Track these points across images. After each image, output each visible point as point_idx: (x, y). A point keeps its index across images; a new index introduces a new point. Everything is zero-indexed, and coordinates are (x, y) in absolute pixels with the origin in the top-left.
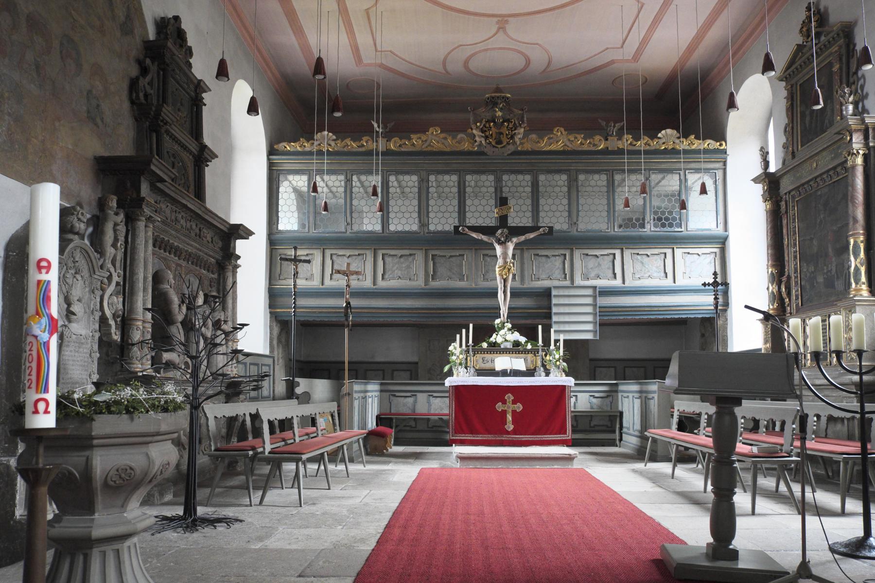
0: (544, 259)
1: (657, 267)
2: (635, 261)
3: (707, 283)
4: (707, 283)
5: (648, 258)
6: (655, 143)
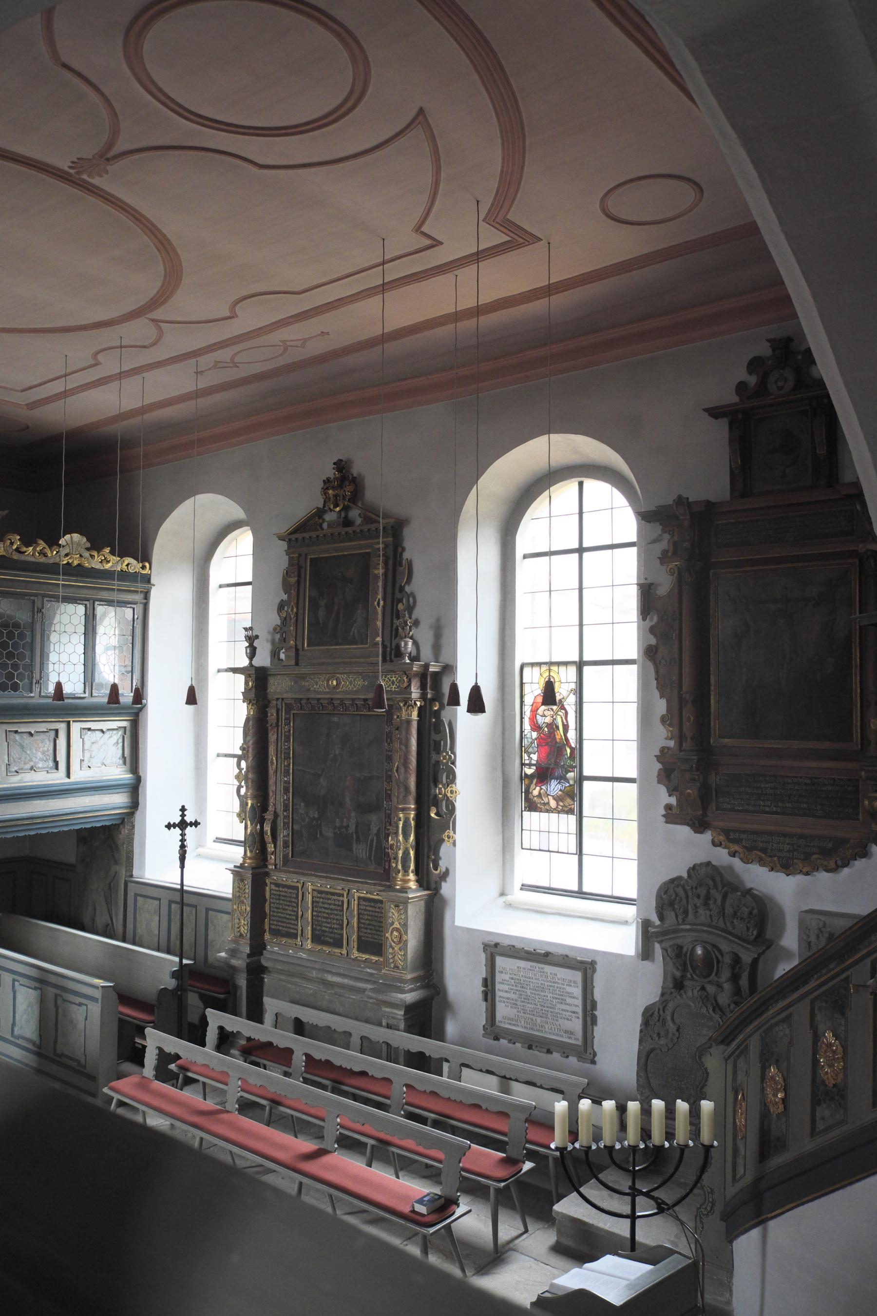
1: (43, 753)
2: (11, 743)
5: (32, 739)
6: (55, 552)
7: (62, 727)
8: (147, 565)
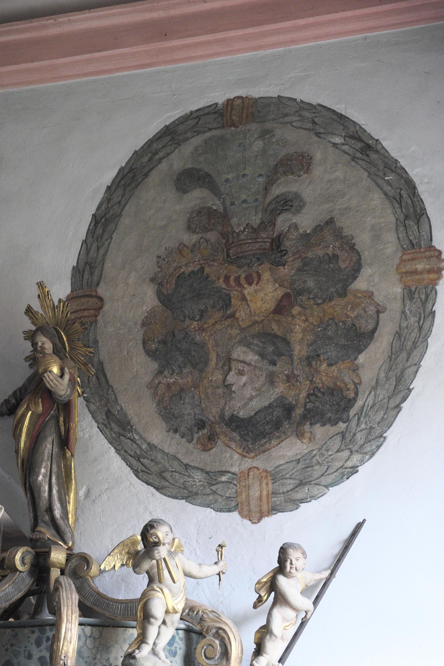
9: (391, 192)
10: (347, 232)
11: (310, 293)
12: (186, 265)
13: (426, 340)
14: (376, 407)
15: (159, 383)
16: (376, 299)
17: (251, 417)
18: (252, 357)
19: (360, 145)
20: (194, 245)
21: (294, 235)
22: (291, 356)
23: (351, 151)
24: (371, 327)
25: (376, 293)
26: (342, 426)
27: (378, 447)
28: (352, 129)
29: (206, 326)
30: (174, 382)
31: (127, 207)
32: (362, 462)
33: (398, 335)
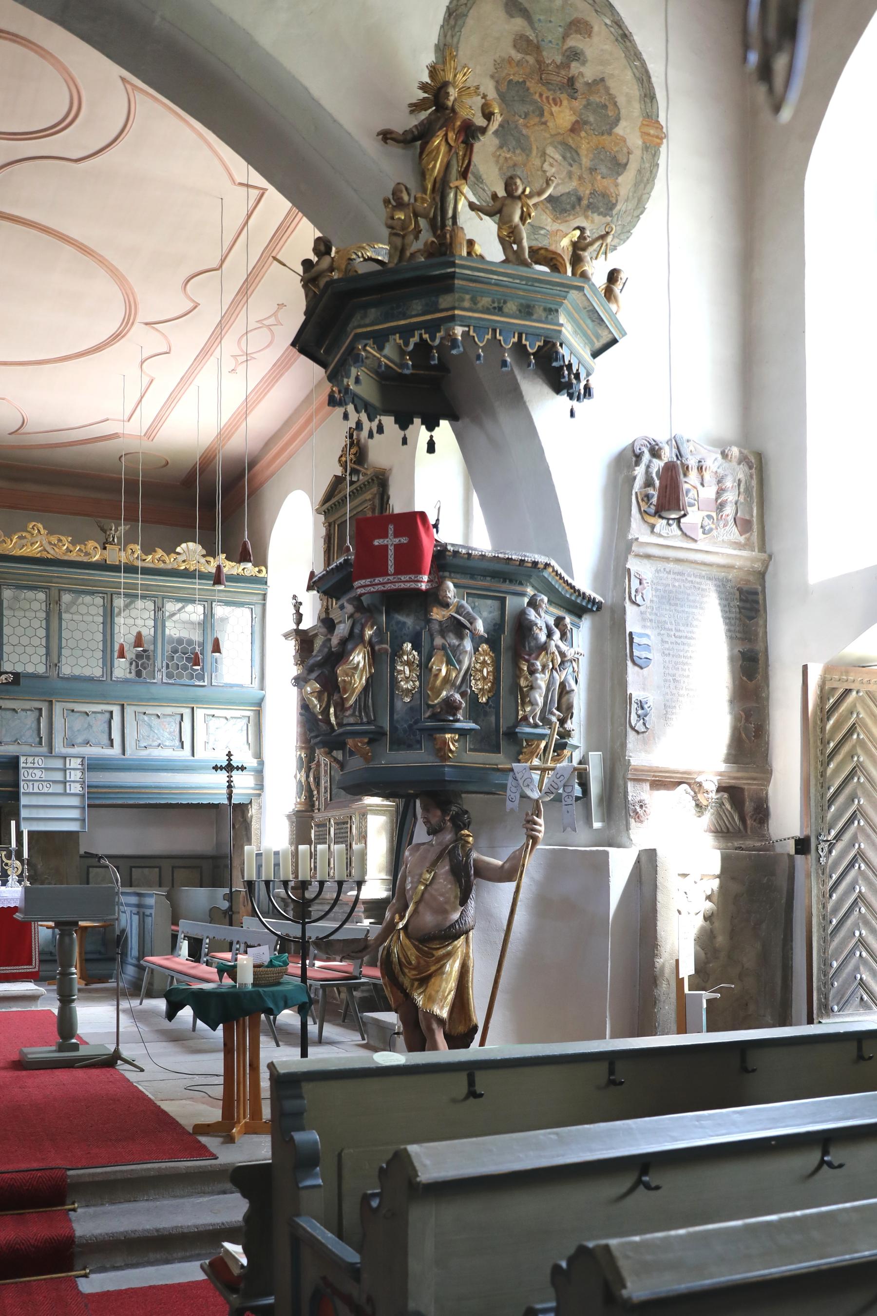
0: (9, 714)
1: (170, 733)
2: (140, 723)
3: (231, 757)
4: (231, 757)
7: (187, 712)
8: (263, 568)
9: (637, 75)
10: (612, 91)
11: (591, 125)
12: (514, 75)
13: (653, 180)
14: (627, 213)
15: (500, 155)
16: (628, 144)
17: (558, 197)
18: (558, 157)
19: (620, 32)
20: (519, 61)
21: (581, 80)
22: (581, 164)
23: (616, 34)
24: (625, 161)
25: (628, 140)
26: (609, 219)
27: (628, 238)
28: (616, 17)
29: (529, 125)
30: (510, 158)
31: (471, 11)
32: (619, 244)
33: (639, 171)
